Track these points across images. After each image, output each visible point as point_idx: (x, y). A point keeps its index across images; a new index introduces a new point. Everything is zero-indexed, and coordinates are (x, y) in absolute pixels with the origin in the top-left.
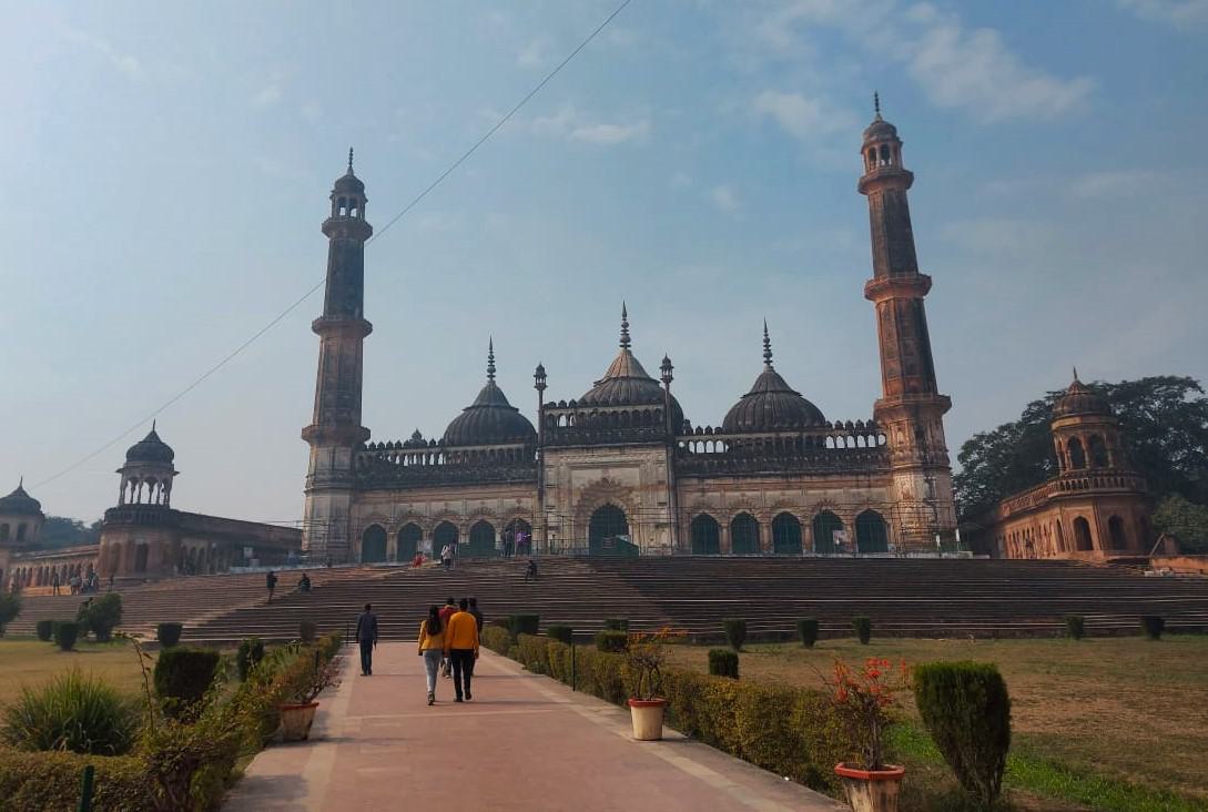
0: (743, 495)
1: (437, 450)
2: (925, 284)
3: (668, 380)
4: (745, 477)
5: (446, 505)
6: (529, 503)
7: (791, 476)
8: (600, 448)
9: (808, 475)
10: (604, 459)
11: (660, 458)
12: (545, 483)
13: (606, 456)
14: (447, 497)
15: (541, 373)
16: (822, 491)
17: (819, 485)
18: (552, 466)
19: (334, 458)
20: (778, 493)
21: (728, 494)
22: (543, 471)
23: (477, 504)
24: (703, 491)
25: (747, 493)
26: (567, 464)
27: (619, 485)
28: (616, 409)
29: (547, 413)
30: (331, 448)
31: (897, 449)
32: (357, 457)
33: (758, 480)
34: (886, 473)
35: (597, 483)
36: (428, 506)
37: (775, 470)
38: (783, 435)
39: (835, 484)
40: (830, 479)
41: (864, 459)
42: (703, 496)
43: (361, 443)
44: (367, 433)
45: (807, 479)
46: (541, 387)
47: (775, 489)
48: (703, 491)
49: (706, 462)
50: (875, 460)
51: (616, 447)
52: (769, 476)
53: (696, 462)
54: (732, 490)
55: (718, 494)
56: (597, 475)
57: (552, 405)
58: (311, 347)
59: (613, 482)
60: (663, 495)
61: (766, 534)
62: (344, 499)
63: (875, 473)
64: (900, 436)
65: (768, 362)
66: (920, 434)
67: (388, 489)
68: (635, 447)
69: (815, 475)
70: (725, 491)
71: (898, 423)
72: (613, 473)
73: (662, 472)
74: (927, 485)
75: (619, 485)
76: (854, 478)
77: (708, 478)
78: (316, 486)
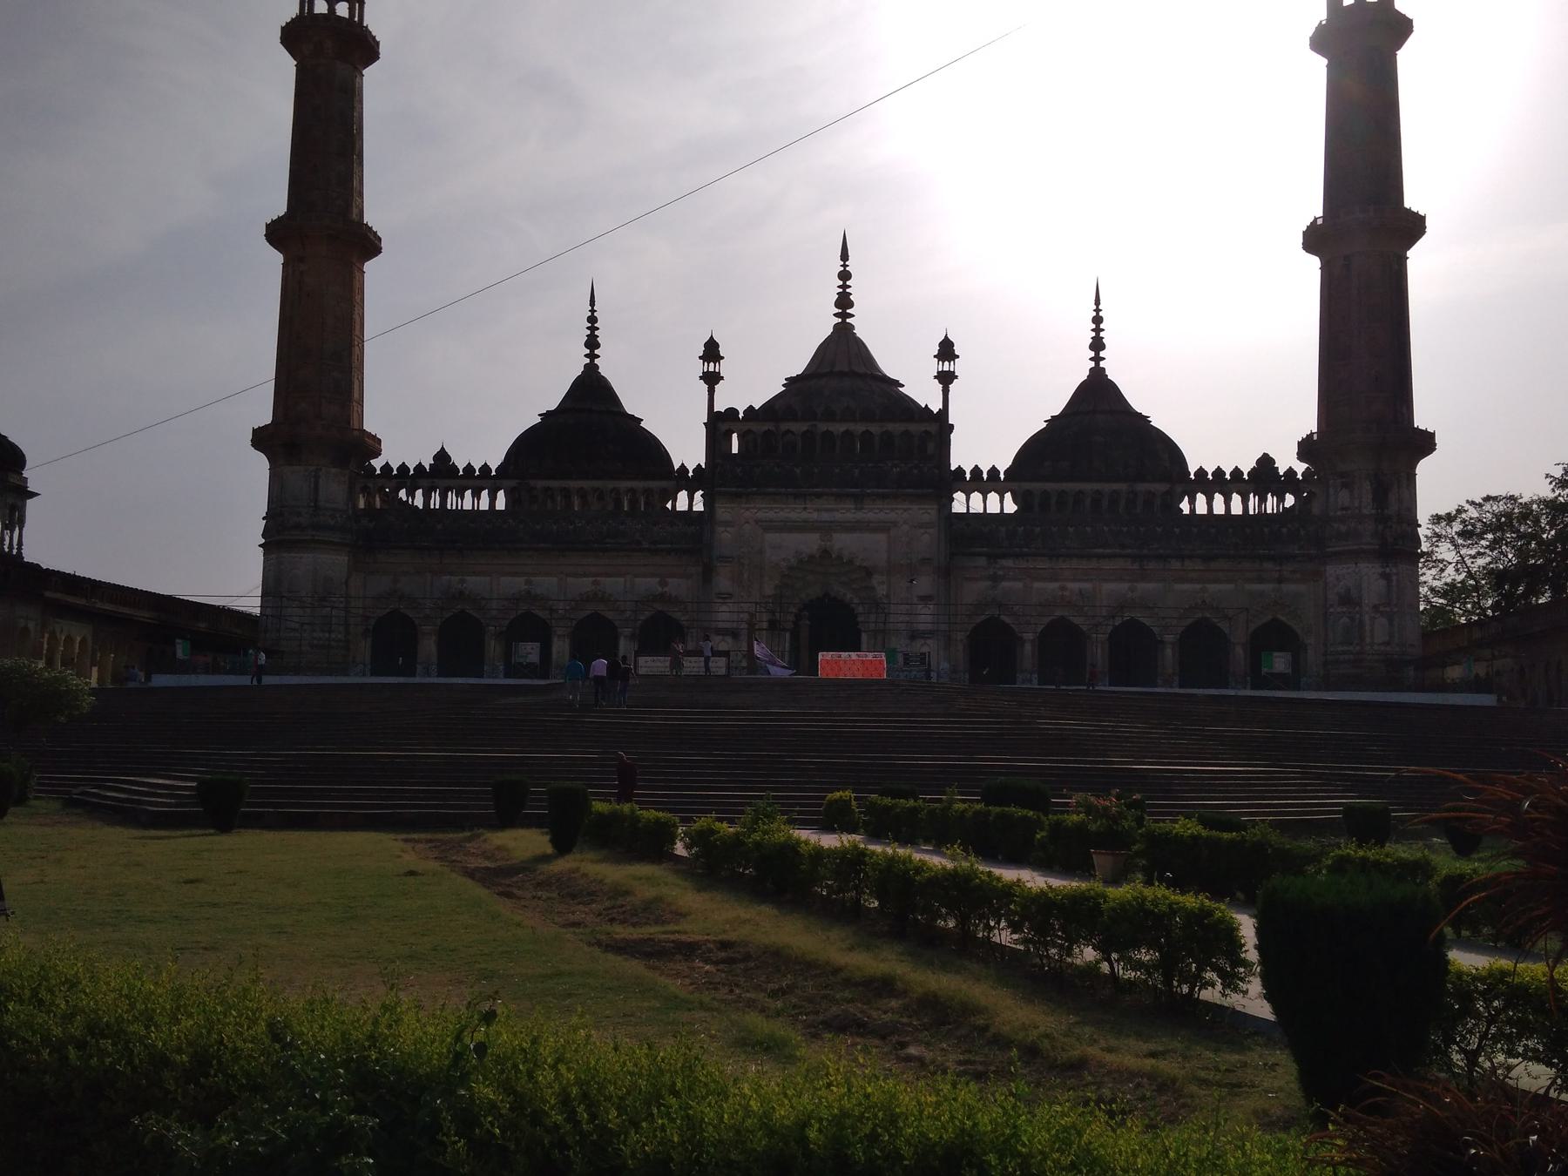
0: (1063, 588)
3: (946, 379)
5: (528, 582)
6: (678, 586)
8: (819, 496)
10: (826, 516)
16: (1198, 586)
18: (727, 524)
20: (1126, 586)
21: (1037, 585)
23: (585, 584)
24: (995, 579)
25: (1070, 585)
26: (757, 522)
27: (851, 562)
28: (852, 427)
35: (811, 557)
36: (496, 584)
38: (1141, 487)
44: (372, 446)
46: (712, 379)
49: (1003, 529)
55: (1019, 585)
56: (810, 543)
59: (840, 557)
60: (924, 584)
61: (1098, 654)
62: (335, 563)
68: (883, 497)
72: (843, 542)
75: (851, 562)
77: (1004, 556)
78: (281, 534)
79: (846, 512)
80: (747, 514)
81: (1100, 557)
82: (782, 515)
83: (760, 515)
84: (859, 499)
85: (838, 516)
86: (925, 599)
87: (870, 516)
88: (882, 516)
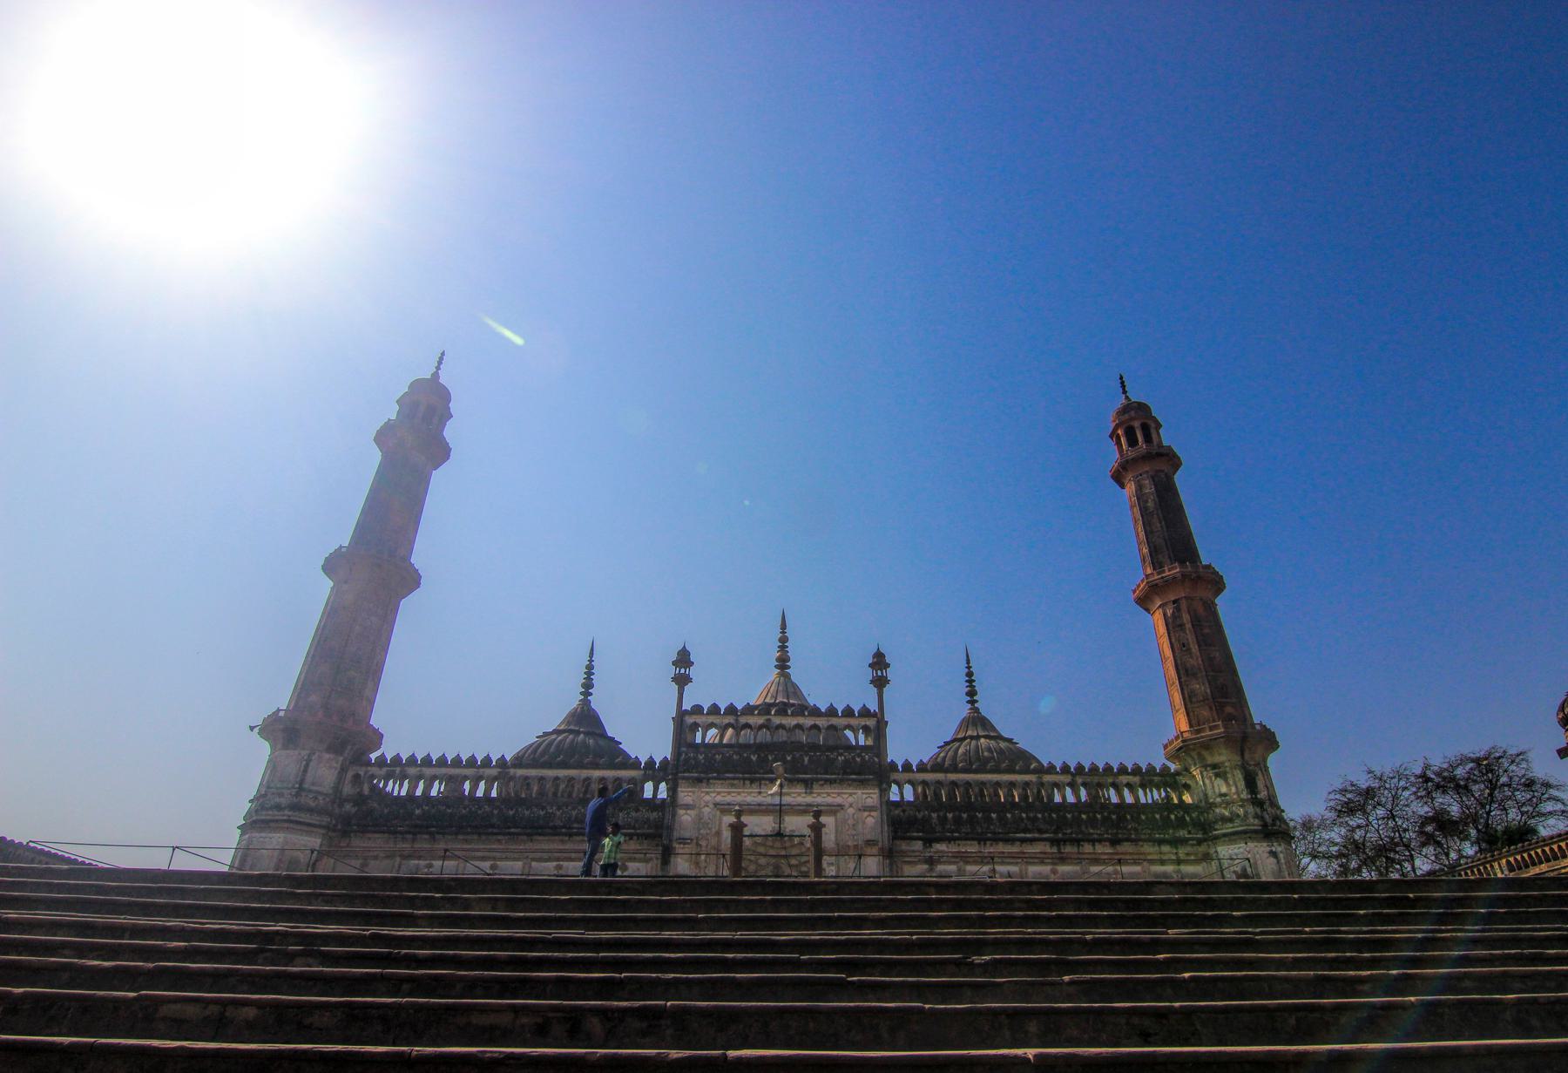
1: (494, 772)
2: (1216, 583)
3: (880, 683)
4: (996, 840)
9: (1089, 841)
11: (870, 802)
12: (676, 835)
15: (683, 659)
18: (687, 807)
19: (305, 771)
20: (1048, 868)
22: (674, 815)
24: (931, 862)
26: (716, 805)
29: (690, 720)
30: (305, 753)
32: (350, 774)
33: (1015, 849)
34: (1200, 842)
37: (1040, 831)
40: (1120, 848)
41: (1166, 820)
42: (931, 870)
43: (360, 758)
44: (377, 738)
45: (1088, 848)
46: (682, 681)
47: (1042, 862)
48: (931, 862)
49: (934, 815)
52: (1032, 840)
53: (920, 816)
54: (975, 863)
55: (953, 868)
57: (697, 709)
58: (317, 593)
65: (972, 702)
66: (1251, 783)
67: (395, 833)
68: (831, 782)
69: (1100, 841)
70: (967, 863)
71: (1214, 766)
73: (871, 823)
74: (1272, 860)
77: (939, 840)
80: (707, 798)
81: (1023, 841)
83: (719, 799)
84: (808, 784)
87: (819, 800)
88: (829, 800)
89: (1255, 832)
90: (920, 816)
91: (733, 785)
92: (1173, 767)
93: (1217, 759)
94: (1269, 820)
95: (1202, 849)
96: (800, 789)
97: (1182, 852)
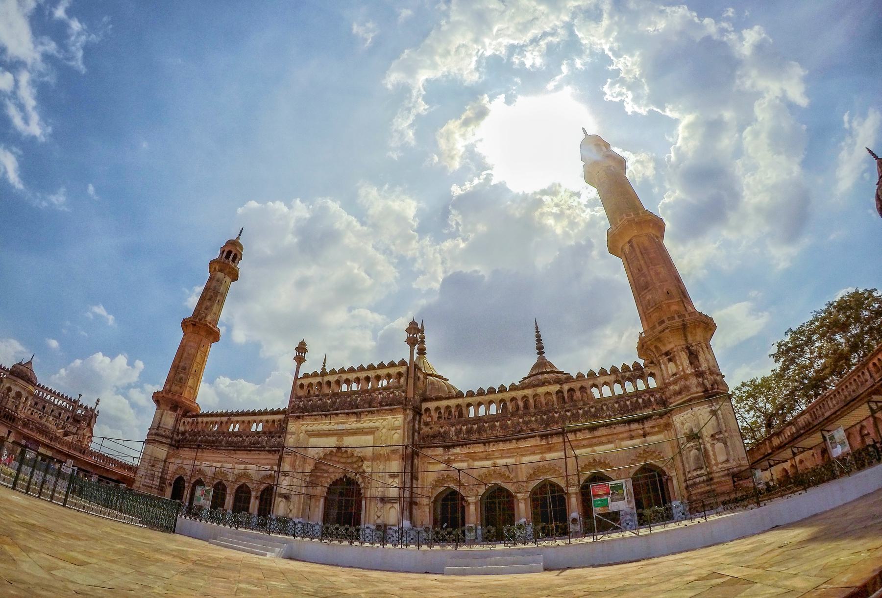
7: (551, 435)
8: (337, 415)
10: (341, 427)
13: (342, 423)
14: (223, 459)
16: (589, 450)
17: (584, 442)
18: (293, 433)
31: (670, 384)
33: (513, 445)
34: (661, 416)
39: (604, 439)
40: (597, 433)
47: (534, 453)
48: (448, 462)
50: (647, 404)
51: (353, 413)
52: (525, 438)
53: (442, 430)
54: (481, 459)
63: (648, 418)
64: (671, 368)
68: (372, 412)
70: (475, 460)
71: (667, 354)
72: (349, 441)
76: (627, 428)
77: (454, 446)
79: (352, 423)
82: (319, 427)
85: (347, 426)
86: (393, 476)
87: (365, 425)
88: (371, 424)
89: (699, 398)
90: (442, 430)
91: (316, 419)
92: (642, 362)
93: (668, 347)
94: (709, 386)
95: (662, 421)
96: (353, 419)
97: (648, 425)
